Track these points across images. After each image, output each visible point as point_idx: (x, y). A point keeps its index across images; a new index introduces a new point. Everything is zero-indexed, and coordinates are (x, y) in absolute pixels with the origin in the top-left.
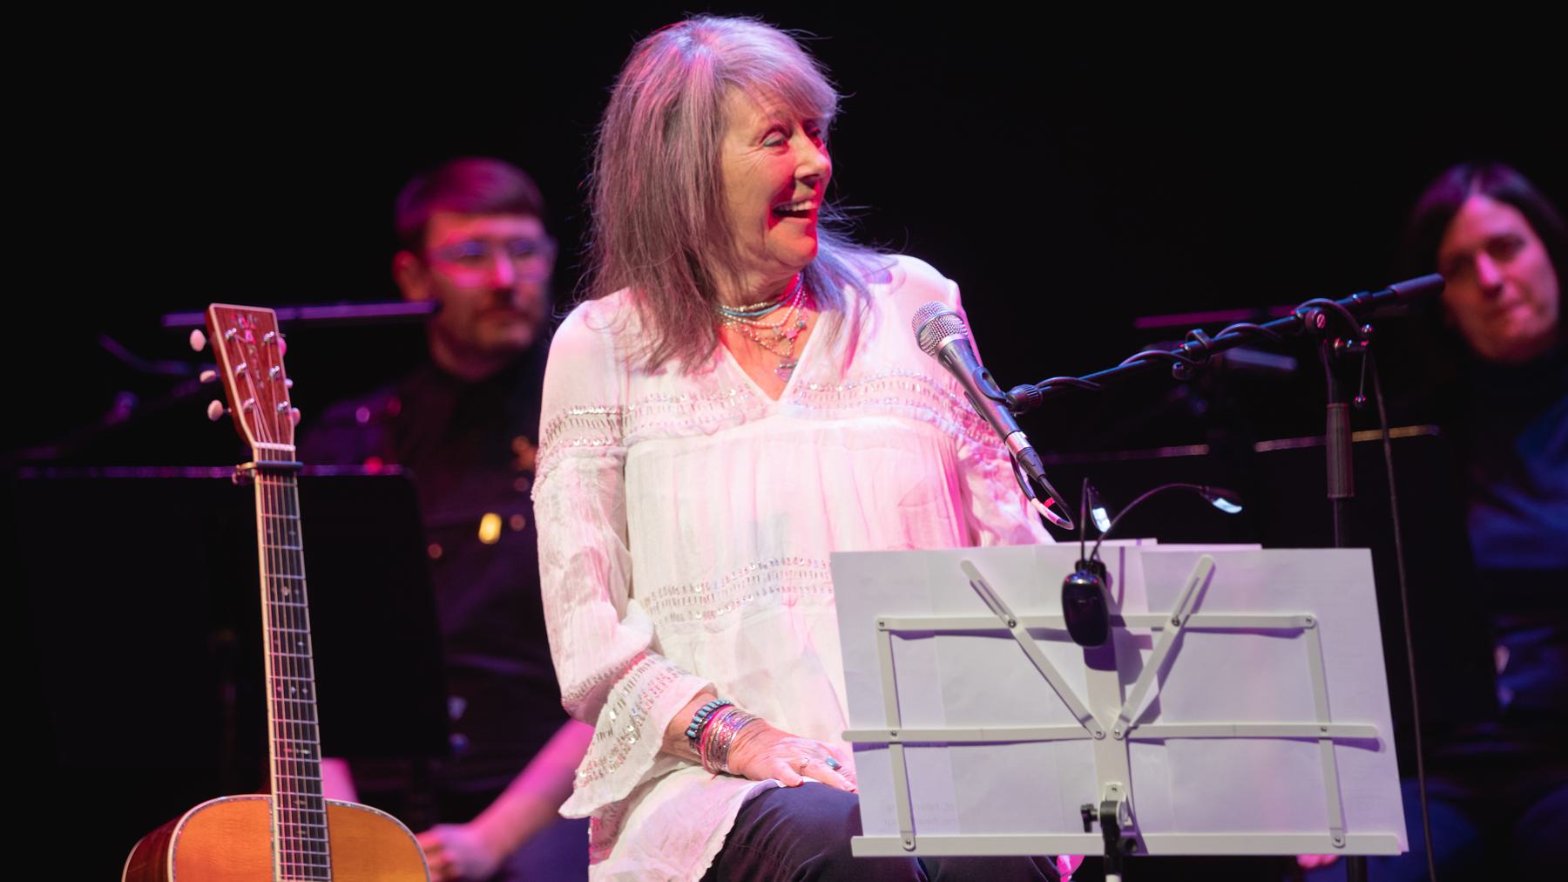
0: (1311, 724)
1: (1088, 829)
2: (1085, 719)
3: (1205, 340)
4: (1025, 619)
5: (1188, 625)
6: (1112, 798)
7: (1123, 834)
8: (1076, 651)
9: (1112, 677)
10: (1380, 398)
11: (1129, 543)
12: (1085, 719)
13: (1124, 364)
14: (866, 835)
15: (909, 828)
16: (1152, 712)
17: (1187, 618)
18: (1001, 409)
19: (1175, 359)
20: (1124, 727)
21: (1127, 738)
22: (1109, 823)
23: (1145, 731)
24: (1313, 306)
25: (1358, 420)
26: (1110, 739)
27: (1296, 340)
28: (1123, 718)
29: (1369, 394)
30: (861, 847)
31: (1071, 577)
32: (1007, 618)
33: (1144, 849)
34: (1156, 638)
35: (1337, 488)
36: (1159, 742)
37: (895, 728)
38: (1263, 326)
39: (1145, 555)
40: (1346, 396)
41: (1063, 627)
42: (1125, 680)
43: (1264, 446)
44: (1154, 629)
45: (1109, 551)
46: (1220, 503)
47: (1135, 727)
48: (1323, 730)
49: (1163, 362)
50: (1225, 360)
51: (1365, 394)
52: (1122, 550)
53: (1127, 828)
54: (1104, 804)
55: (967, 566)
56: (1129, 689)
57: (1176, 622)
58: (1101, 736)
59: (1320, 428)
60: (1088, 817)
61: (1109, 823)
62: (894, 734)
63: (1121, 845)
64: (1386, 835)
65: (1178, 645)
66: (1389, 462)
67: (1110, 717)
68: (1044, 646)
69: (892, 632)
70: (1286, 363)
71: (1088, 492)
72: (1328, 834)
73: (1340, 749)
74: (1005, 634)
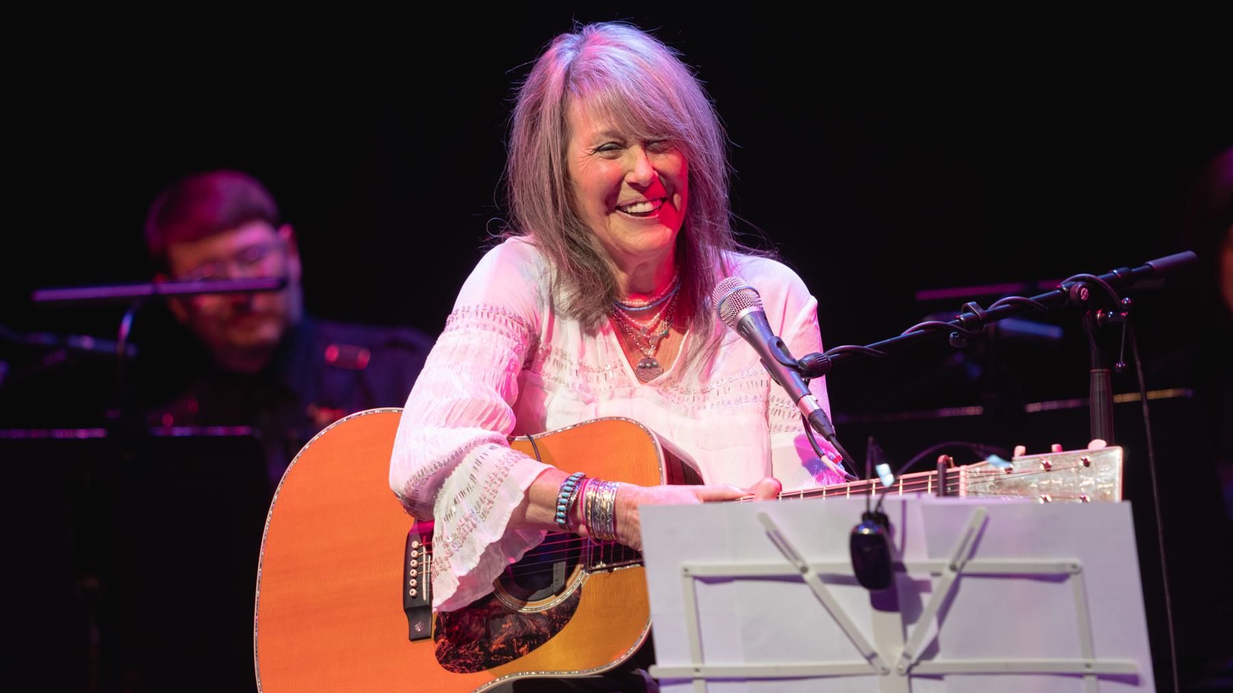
0: (1076, 661)
2: (871, 657)
3: (979, 312)
4: (817, 566)
5: (966, 570)
8: (861, 595)
9: (895, 618)
10: (1139, 364)
12: (871, 657)
13: (904, 334)
16: (932, 650)
17: (963, 565)
18: (794, 374)
19: (951, 329)
20: (907, 663)
21: (910, 674)
23: (925, 667)
24: (1077, 280)
25: (1118, 383)
26: (894, 674)
28: (906, 655)
31: (858, 527)
32: (800, 564)
34: (935, 583)
36: (938, 677)
37: (698, 665)
38: (1031, 299)
39: (926, 508)
41: (849, 572)
43: (1033, 407)
45: (892, 505)
47: (916, 664)
48: (1088, 666)
49: (943, 330)
50: (997, 329)
52: (904, 503)
55: (764, 518)
56: (911, 629)
57: (953, 568)
58: (886, 672)
62: (697, 670)
66: (1147, 422)
68: (834, 591)
69: (696, 578)
70: (1054, 332)
71: (872, 449)
73: (1103, 684)
74: (797, 579)
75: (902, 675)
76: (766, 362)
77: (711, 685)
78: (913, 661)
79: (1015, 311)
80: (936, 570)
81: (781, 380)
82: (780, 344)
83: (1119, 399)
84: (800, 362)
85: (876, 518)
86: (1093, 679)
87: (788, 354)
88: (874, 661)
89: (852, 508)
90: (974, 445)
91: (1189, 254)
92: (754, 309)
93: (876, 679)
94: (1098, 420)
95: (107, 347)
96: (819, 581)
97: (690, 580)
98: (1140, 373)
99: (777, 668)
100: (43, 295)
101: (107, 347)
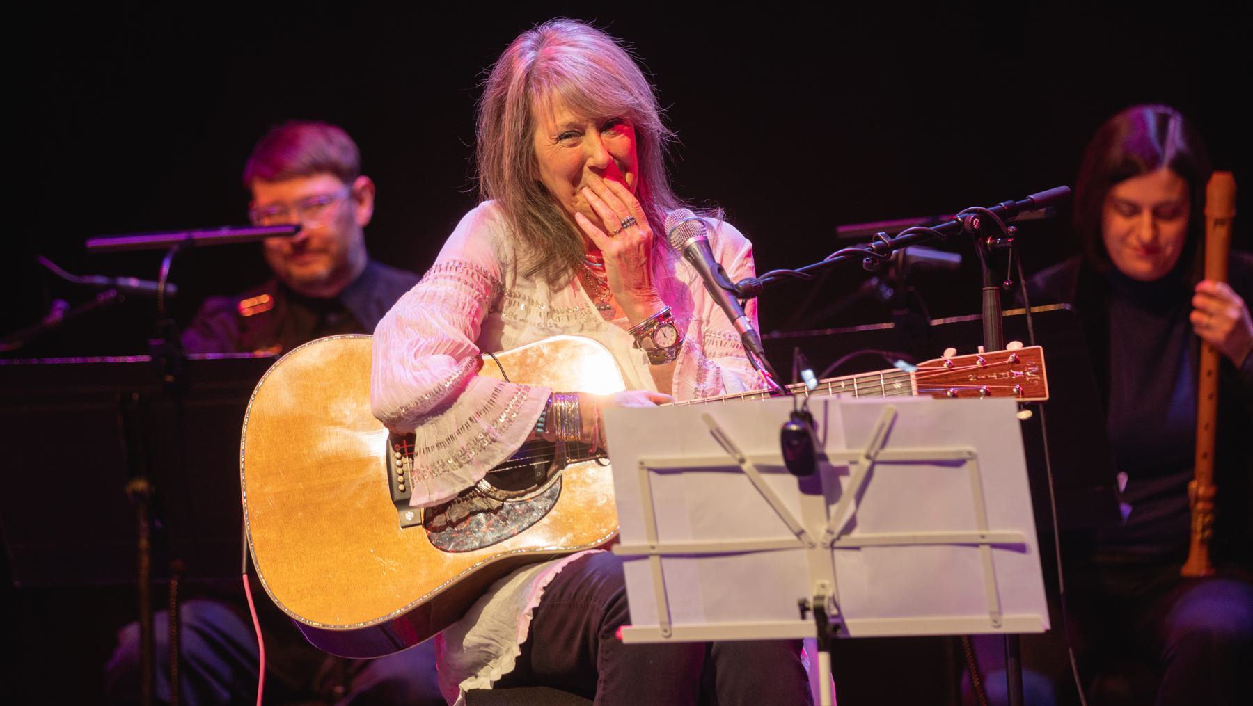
0: (973, 533)
1: (803, 617)
2: (800, 534)
4: (752, 457)
5: (879, 458)
6: (822, 593)
7: (832, 621)
8: (792, 481)
9: (820, 500)
12: (800, 534)
13: (827, 260)
15: (666, 619)
16: (851, 525)
17: (876, 454)
19: (864, 254)
20: (830, 538)
21: (832, 546)
22: (820, 613)
25: (1007, 300)
26: (819, 549)
28: (829, 532)
30: (628, 635)
31: (787, 424)
32: (738, 456)
33: (846, 631)
36: (857, 548)
37: (654, 543)
39: (844, 407)
40: (997, 281)
41: (780, 462)
42: (831, 500)
43: (935, 322)
48: (983, 537)
50: (905, 256)
52: (826, 402)
53: (834, 617)
54: (819, 598)
55: (707, 418)
57: (868, 457)
58: (812, 546)
59: (978, 308)
60: (803, 608)
61: (820, 613)
62: (653, 548)
63: (829, 629)
64: (1031, 617)
65: (869, 475)
66: (1031, 331)
67: (819, 531)
68: (768, 479)
69: (650, 469)
70: (955, 258)
71: (798, 357)
72: (987, 617)
73: (997, 552)
74: (736, 470)
76: (708, 284)
77: (665, 561)
78: (835, 536)
79: (921, 239)
80: (853, 459)
81: (718, 299)
82: (721, 269)
83: (1008, 313)
84: (737, 286)
85: (802, 416)
86: (987, 548)
87: (727, 280)
88: (802, 537)
89: (783, 407)
90: (884, 353)
91: (1064, 188)
93: (805, 552)
95: (150, 286)
97: (645, 472)
99: (721, 545)
100: (92, 244)
101: (150, 286)
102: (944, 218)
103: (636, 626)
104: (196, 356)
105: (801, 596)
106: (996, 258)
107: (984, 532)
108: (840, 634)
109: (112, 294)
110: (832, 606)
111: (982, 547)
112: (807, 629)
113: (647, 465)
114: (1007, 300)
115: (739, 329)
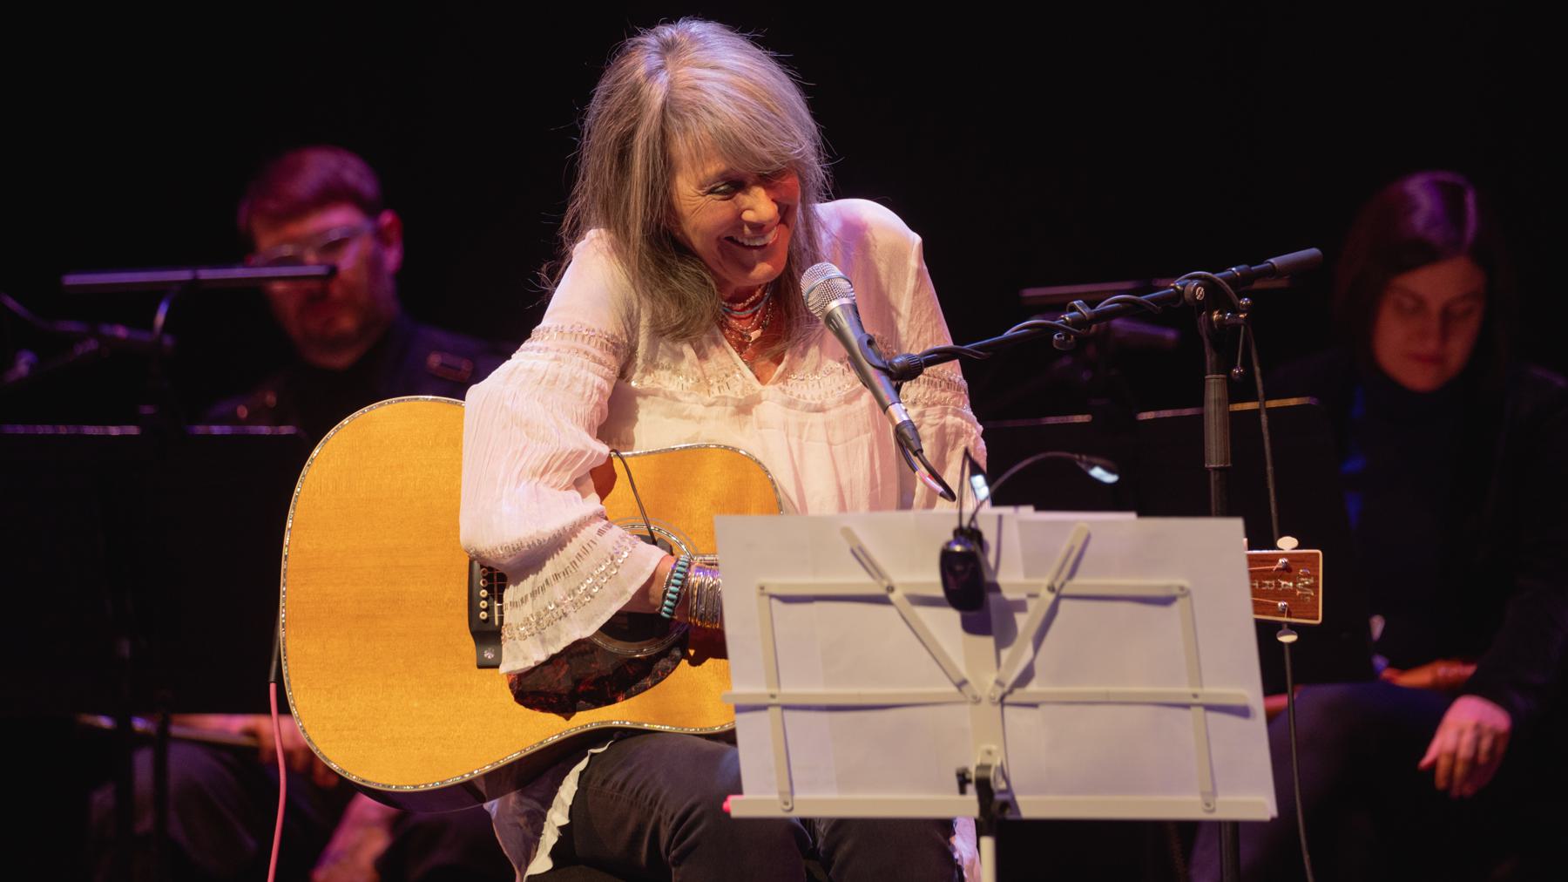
0: (1183, 690)
1: (963, 791)
2: (964, 682)
3: (1086, 311)
4: (903, 585)
5: (1065, 591)
6: (987, 761)
7: (998, 797)
8: (953, 616)
9: (988, 642)
10: (1257, 369)
11: (1007, 511)
12: (961, 685)
13: (1008, 333)
14: (747, 796)
15: (787, 788)
16: (1026, 676)
17: (1062, 585)
19: (1056, 329)
20: (999, 691)
22: (984, 786)
25: (1239, 390)
26: (985, 704)
27: (1179, 312)
28: (999, 683)
29: (1247, 364)
30: (737, 807)
31: (949, 544)
32: (886, 583)
33: (1017, 810)
34: (1032, 604)
35: (1216, 454)
36: (1034, 705)
37: (774, 691)
39: (1022, 524)
40: (1225, 367)
41: (939, 592)
44: (1033, 596)
46: (1097, 472)
48: (1195, 696)
51: (1243, 366)
52: (1000, 518)
53: (1002, 792)
54: (981, 767)
55: (847, 533)
56: (1005, 653)
57: (1051, 589)
59: (1199, 401)
60: (963, 780)
61: (984, 786)
62: (773, 696)
63: (995, 808)
64: (1254, 800)
66: (1265, 432)
67: (986, 682)
68: (925, 614)
69: (772, 596)
70: (1170, 335)
72: (1197, 798)
73: (1212, 716)
74: (882, 600)
75: (994, 704)
77: (789, 714)
78: (1006, 689)
80: (1034, 591)
85: (969, 534)
86: (1201, 710)
88: (964, 688)
92: (846, 301)
93: (968, 707)
94: (1212, 427)
96: (907, 604)
97: (766, 598)
98: (1259, 380)
99: (859, 695)
100: (72, 280)
102: (1162, 282)
103: (748, 795)
104: (200, 429)
105: (960, 765)
106: (1224, 338)
107: (1197, 690)
108: (1009, 815)
109: (92, 345)
110: (1000, 779)
111: (1194, 709)
112: (965, 808)
113: (768, 590)
114: (1239, 390)
115: (892, 419)
